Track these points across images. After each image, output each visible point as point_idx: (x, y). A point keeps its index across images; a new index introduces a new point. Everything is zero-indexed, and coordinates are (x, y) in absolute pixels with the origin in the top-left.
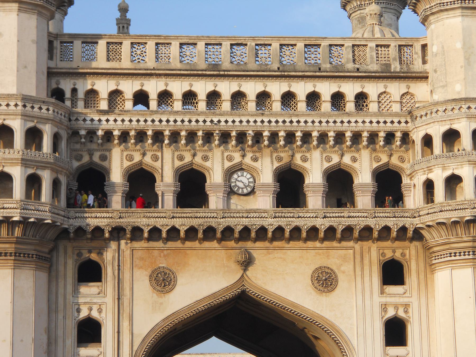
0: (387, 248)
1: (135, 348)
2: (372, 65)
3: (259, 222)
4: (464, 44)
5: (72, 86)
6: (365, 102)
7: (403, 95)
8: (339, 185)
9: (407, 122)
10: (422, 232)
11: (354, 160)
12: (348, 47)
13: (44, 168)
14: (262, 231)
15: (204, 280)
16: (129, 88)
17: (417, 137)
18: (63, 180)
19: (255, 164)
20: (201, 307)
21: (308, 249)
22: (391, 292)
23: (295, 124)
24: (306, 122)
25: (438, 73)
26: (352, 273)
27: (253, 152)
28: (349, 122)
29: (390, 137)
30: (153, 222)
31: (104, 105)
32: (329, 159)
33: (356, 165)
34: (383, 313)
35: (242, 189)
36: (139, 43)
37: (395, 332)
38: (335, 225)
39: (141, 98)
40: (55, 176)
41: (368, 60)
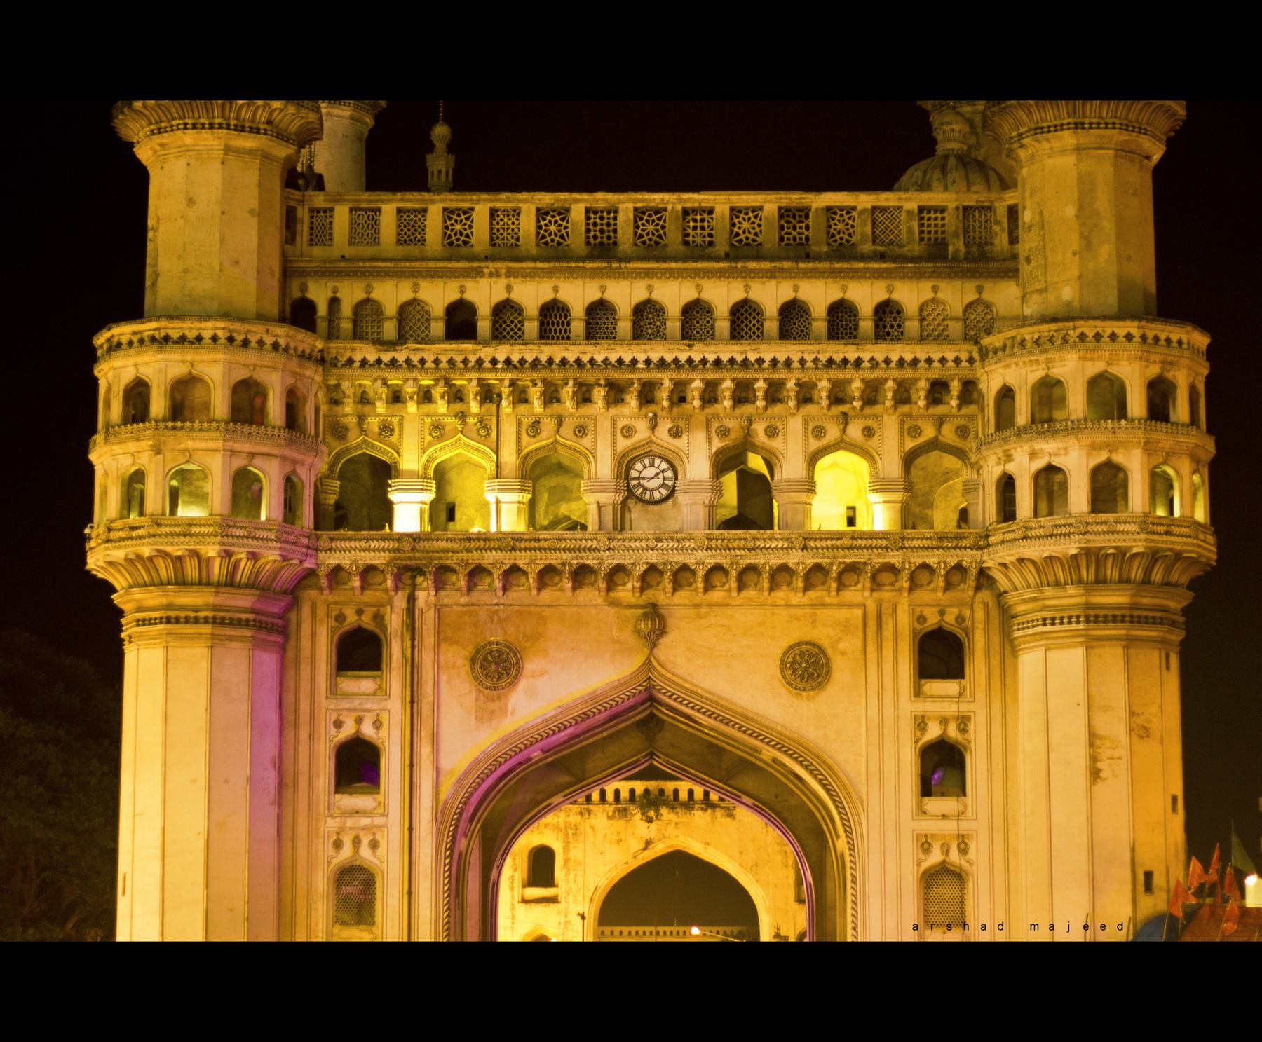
1: (443, 797)
2: (910, 247)
3: (678, 558)
4: (1081, 208)
5: (330, 295)
6: (895, 319)
7: (969, 305)
10: (997, 574)
12: (865, 210)
19: (676, 442)
22: (935, 692)
25: (1033, 264)
26: (859, 655)
27: (673, 419)
29: (938, 390)
34: (918, 733)
35: (652, 490)
36: (458, 209)
38: (825, 562)
41: (904, 235)
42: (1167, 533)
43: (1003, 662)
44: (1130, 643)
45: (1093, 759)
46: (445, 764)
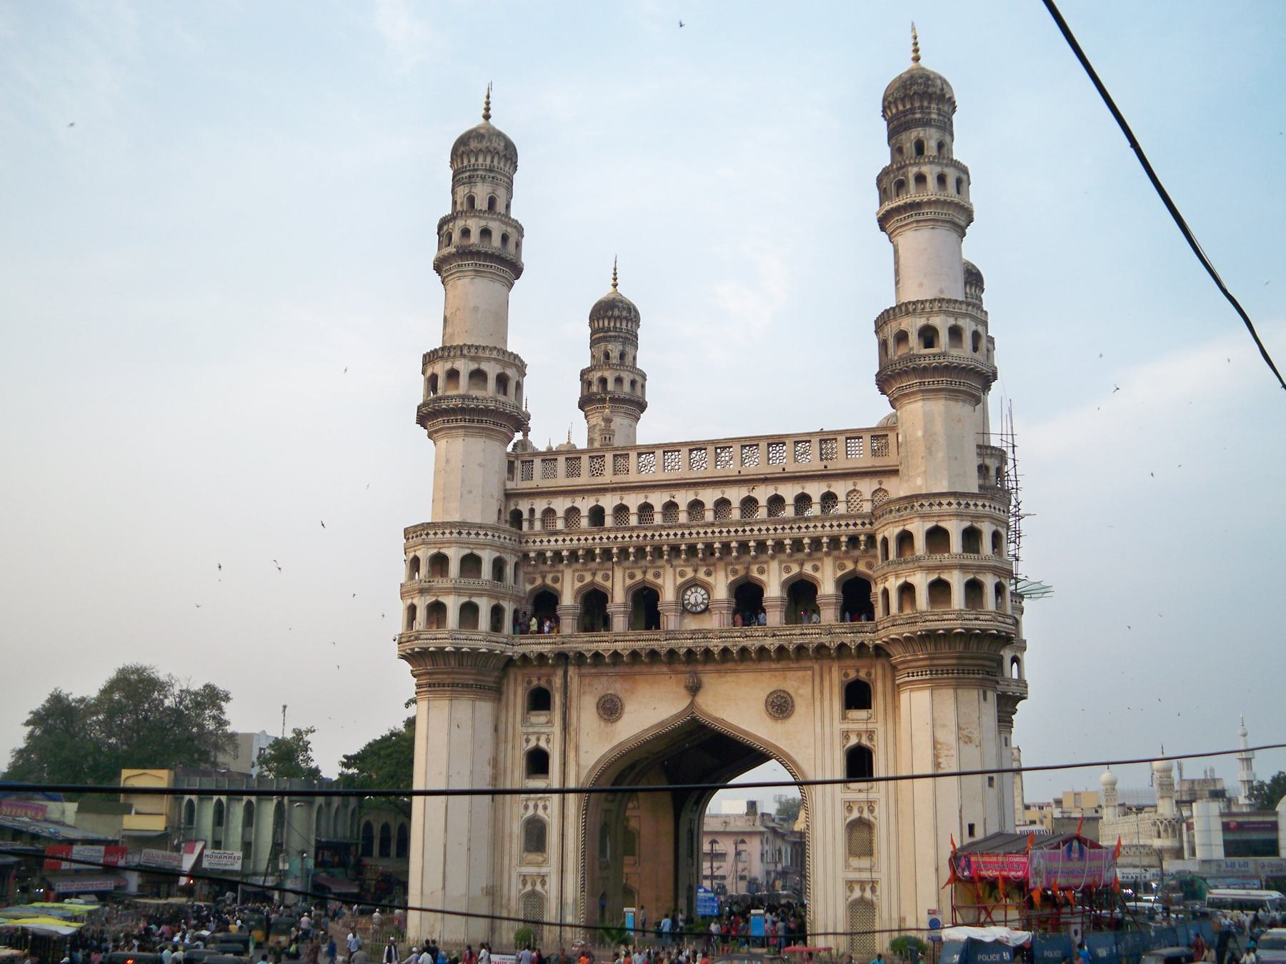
0: (850, 667)
3: (703, 643)
4: (925, 432)
8: (801, 595)
9: (871, 524)
11: (816, 569)
13: (480, 595)
14: (707, 652)
15: (651, 709)
16: (585, 505)
17: (879, 538)
18: (509, 608)
20: (648, 736)
21: (762, 671)
23: (748, 533)
24: (760, 530)
28: (807, 527)
29: (853, 540)
30: (594, 647)
31: (560, 525)
32: (788, 569)
33: (818, 575)
37: (859, 764)
38: (786, 644)
39: (597, 515)
40: (494, 602)
42: (977, 619)
43: (894, 698)
44: (956, 687)
45: (936, 756)
46: (582, 763)
